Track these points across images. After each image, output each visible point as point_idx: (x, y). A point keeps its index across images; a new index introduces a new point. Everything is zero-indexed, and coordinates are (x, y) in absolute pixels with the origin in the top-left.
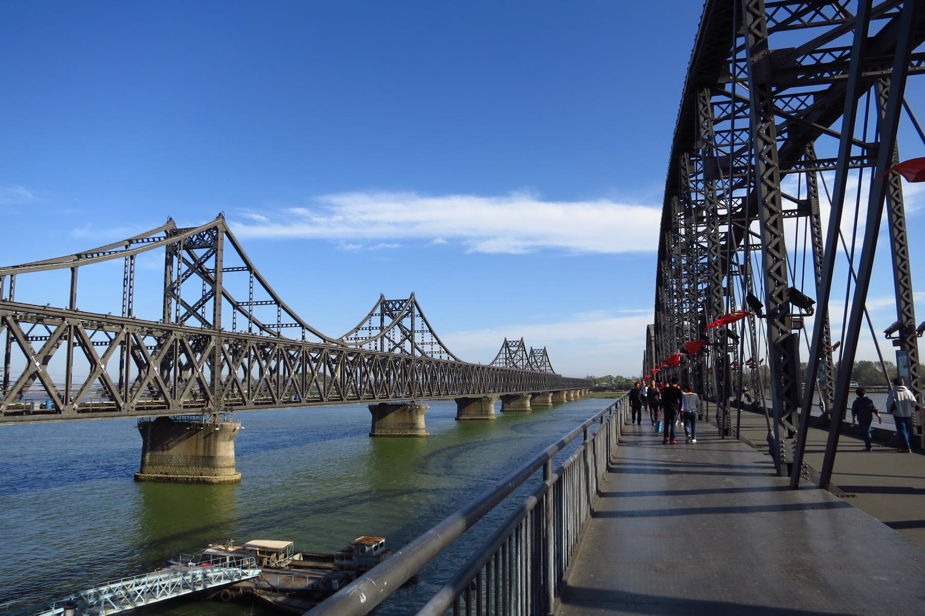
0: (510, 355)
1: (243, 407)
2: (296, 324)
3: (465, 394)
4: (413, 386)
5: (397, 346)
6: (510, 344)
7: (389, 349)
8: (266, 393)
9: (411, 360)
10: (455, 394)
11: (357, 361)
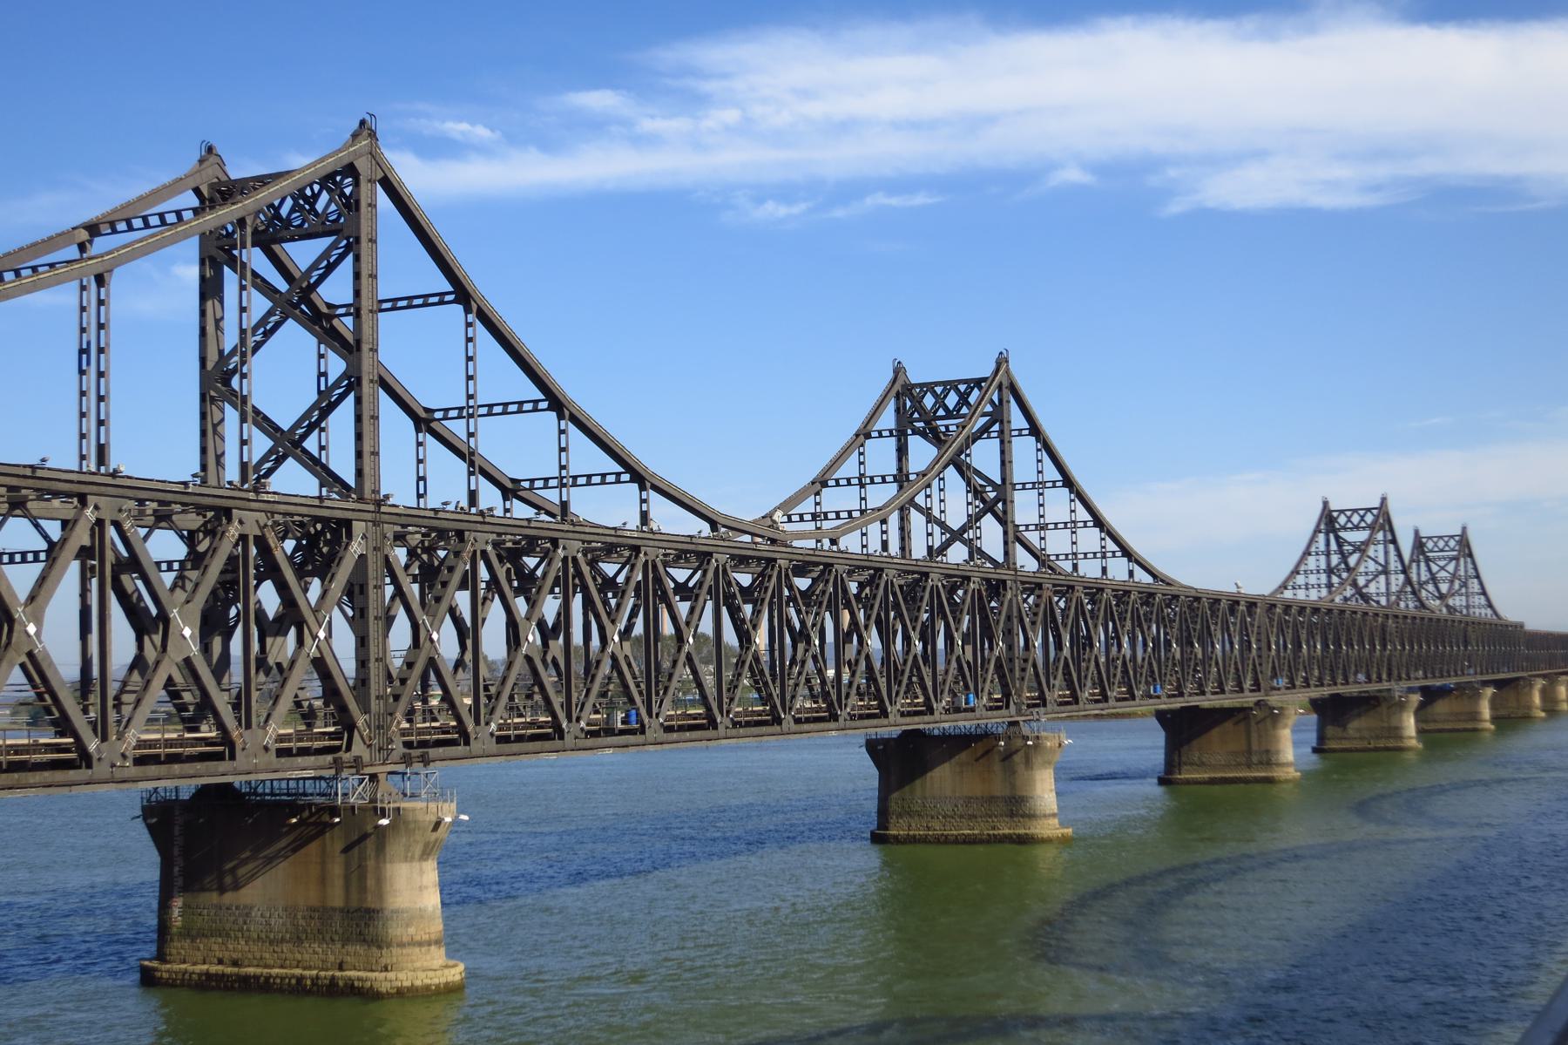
0: (1344, 557)
1: (460, 750)
2: (618, 474)
3: (1190, 695)
4: (1011, 671)
5: (956, 536)
6: (1342, 520)
7: (930, 548)
8: (529, 703)
9: (1004, 582)
10: (1158, 697)
11: (824, 592)
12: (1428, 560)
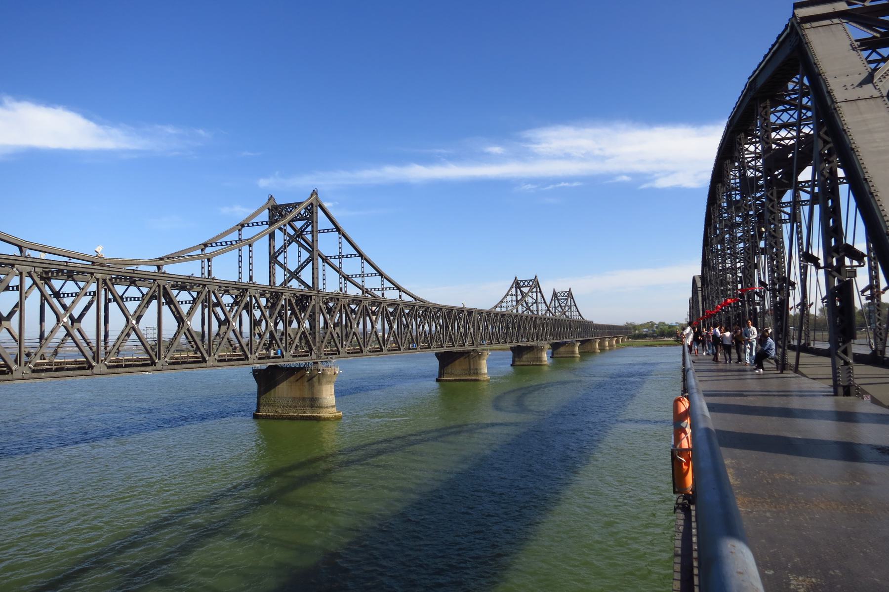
3: (434, 348)
12: (558, 300)
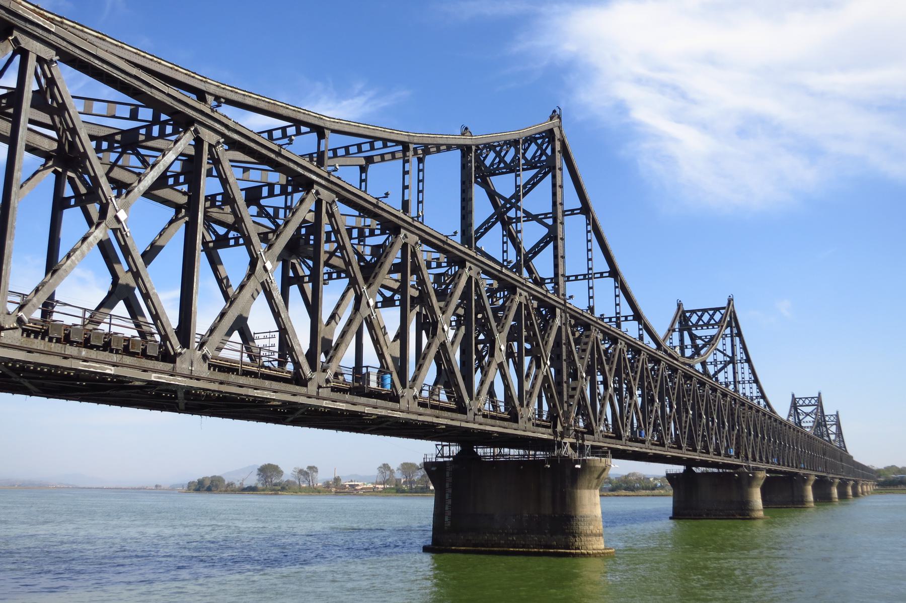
6: (694, 319)
